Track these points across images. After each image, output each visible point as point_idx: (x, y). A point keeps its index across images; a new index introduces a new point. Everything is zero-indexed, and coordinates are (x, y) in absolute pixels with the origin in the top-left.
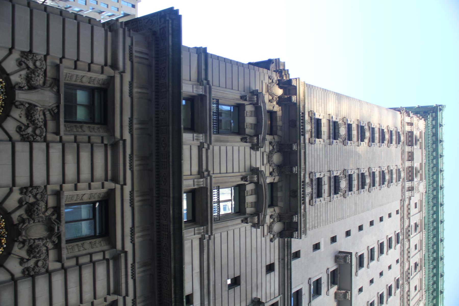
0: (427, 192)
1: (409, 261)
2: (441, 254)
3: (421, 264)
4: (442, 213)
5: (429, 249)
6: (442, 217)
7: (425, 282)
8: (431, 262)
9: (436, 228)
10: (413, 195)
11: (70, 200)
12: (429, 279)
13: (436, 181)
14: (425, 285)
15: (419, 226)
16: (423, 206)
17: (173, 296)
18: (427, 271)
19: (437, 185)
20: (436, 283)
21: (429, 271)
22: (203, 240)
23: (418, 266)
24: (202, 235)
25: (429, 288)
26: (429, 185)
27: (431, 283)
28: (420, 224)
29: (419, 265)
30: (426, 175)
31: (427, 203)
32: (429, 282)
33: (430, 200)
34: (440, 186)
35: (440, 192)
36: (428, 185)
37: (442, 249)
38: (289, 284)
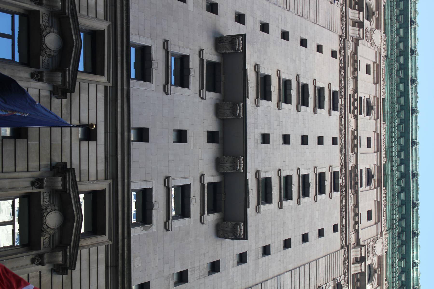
0: (389, 56)
1: (357, 154)
2: (412, 168)
3: (378, 176)
4: (413, 95)
5: (392, 157)
6: (414, 103)
7: (386, 214)
8: (396, 179)
9: (405, 122)
10: (361, 36)
12: (393, 210)
13: (404, 39)
14: (386, 219)
15: (375, 108)
16: (382, 79)
18: (389, 194)
19: (406, 46)
20: (405, 217)
21: (393, 195)
23: (373, 178)
25: (393, 225)
26: (391, 45)
27: (397, 217)
28: (376, 104)
29: (376, 177)
30: (387, 26)
31: (388, 76)
32: (393, 215)
33: (394, 72)
34: (411, 48)
35: (411, 58)
36: (390, 44)
37: (414, 159)
38: (124, 8)
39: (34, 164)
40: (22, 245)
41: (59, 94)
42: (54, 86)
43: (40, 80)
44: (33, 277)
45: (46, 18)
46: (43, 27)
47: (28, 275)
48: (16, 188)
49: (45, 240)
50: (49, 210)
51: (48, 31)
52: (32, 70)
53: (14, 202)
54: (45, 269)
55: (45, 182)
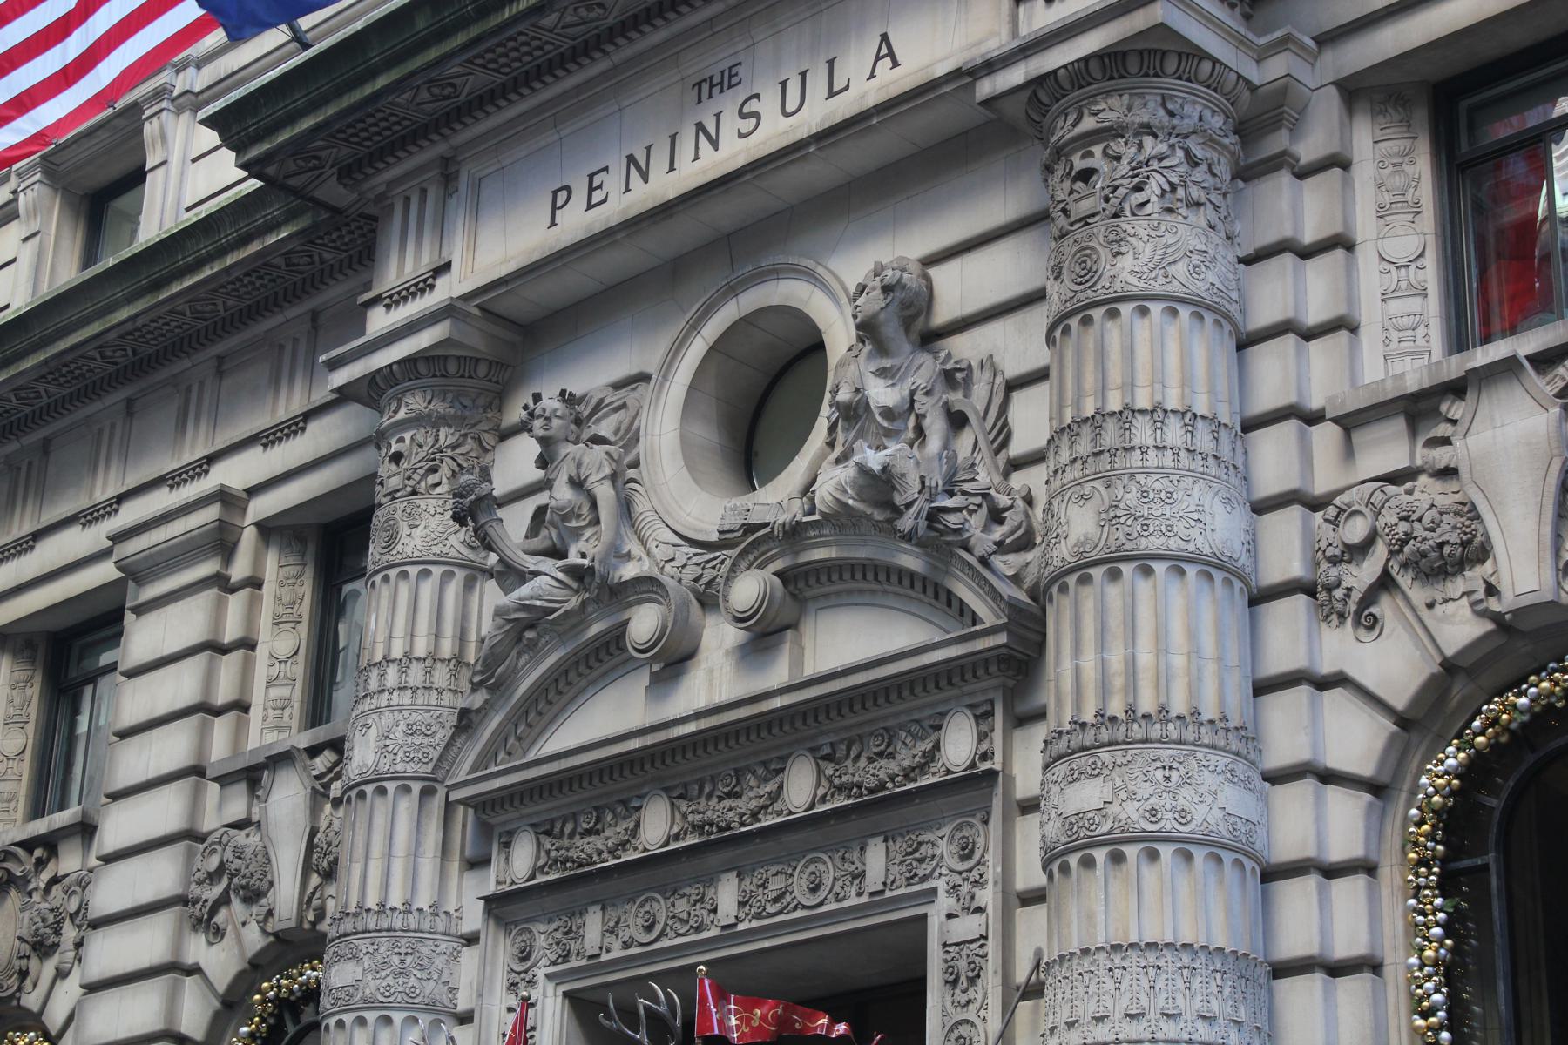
11: (13, 805)
17: (207, 272)
22: (199, 93)
24: (179, 112)
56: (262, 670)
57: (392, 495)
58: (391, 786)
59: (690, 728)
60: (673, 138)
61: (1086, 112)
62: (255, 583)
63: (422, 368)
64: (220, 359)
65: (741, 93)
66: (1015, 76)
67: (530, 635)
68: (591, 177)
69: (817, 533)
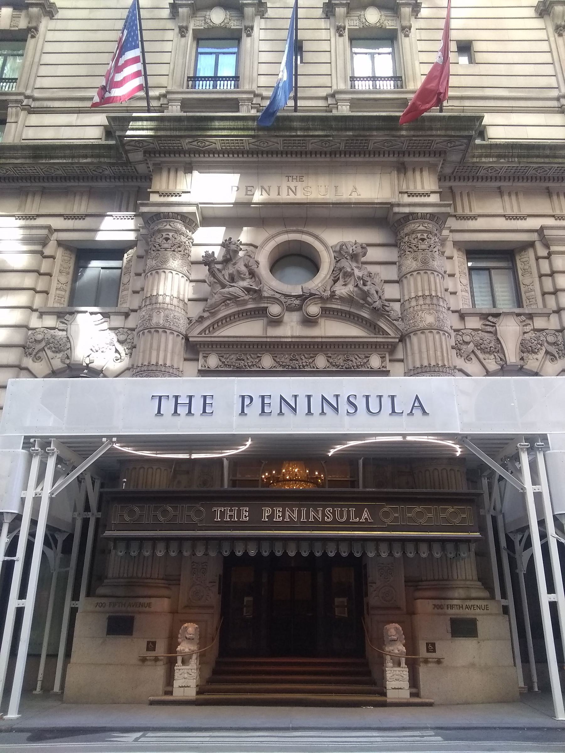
22: (32, 108)
24: (23, 110)
39: (324, 34)
40: (393, 46)
41: (263, 11)
42: (256, 15)
43: (252, 28)
44: (420, 37)
45: (198, 23)
46: (206, 26)
47: (418, 40)
48: (345, 51)
49: (390, 24)
50: (364, 20)
51: (209, 21)
52: (244, 35)
53: (356, 53)
54: (415, 24)
55: (340, 24)
56: (54, 284)
57: (166, 249)
58: (168, 331)
59: (290, 340)
60: (279, 188)
61: (421, 225)
62: (53, 257)
63: (179, 217)
64: (44, 188)
65: (304, 184)
66: (407, 210)
67: (228, 302)
68: (247, 187)
69: (335, 301)
